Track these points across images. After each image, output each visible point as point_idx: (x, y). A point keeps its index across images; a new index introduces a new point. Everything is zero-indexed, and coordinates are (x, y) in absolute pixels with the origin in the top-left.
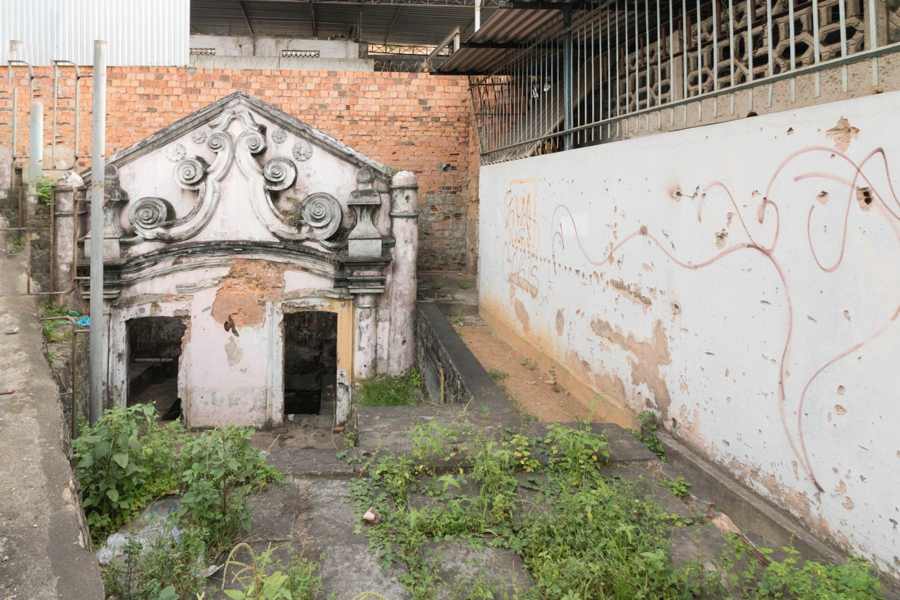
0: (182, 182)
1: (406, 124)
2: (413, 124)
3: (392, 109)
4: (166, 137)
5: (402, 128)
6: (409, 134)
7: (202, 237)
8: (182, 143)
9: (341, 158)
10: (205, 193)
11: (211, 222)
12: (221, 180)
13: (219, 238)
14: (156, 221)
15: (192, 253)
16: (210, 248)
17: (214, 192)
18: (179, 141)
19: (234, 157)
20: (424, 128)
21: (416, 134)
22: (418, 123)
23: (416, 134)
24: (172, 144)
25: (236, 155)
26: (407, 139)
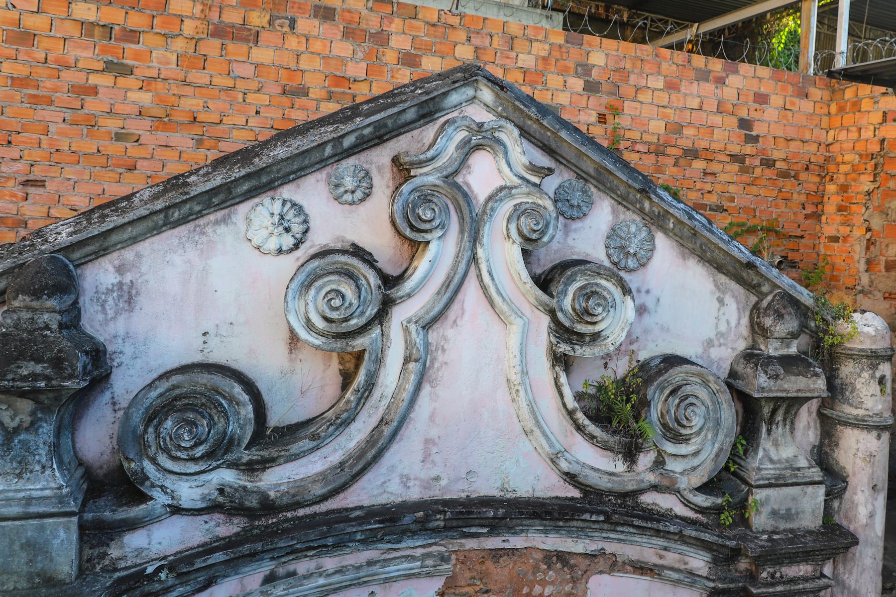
0: (309, 325)
1: (715, 167)
2: (728, 167)
3: (688, 132)
4: (249, 175)
5: (705, 174)
6: (719, 188)
7: (366, 493)
8: (298, 199)
9: (720, 268)
10: (379, 361)
11: (395, 447)
12: (427, 326)
13: (415, 494)
14: (220, 451)
15: (334, 546)
16: (391, 522)
17: (407, 360)
18: (287, 192)
19: (474, 258)
20: (745, 178)
21: (732, 188)
22: (736, 167)
23: (732, 188)
24: (266, 199)
25: (480, 252)
26: (713, 199)
